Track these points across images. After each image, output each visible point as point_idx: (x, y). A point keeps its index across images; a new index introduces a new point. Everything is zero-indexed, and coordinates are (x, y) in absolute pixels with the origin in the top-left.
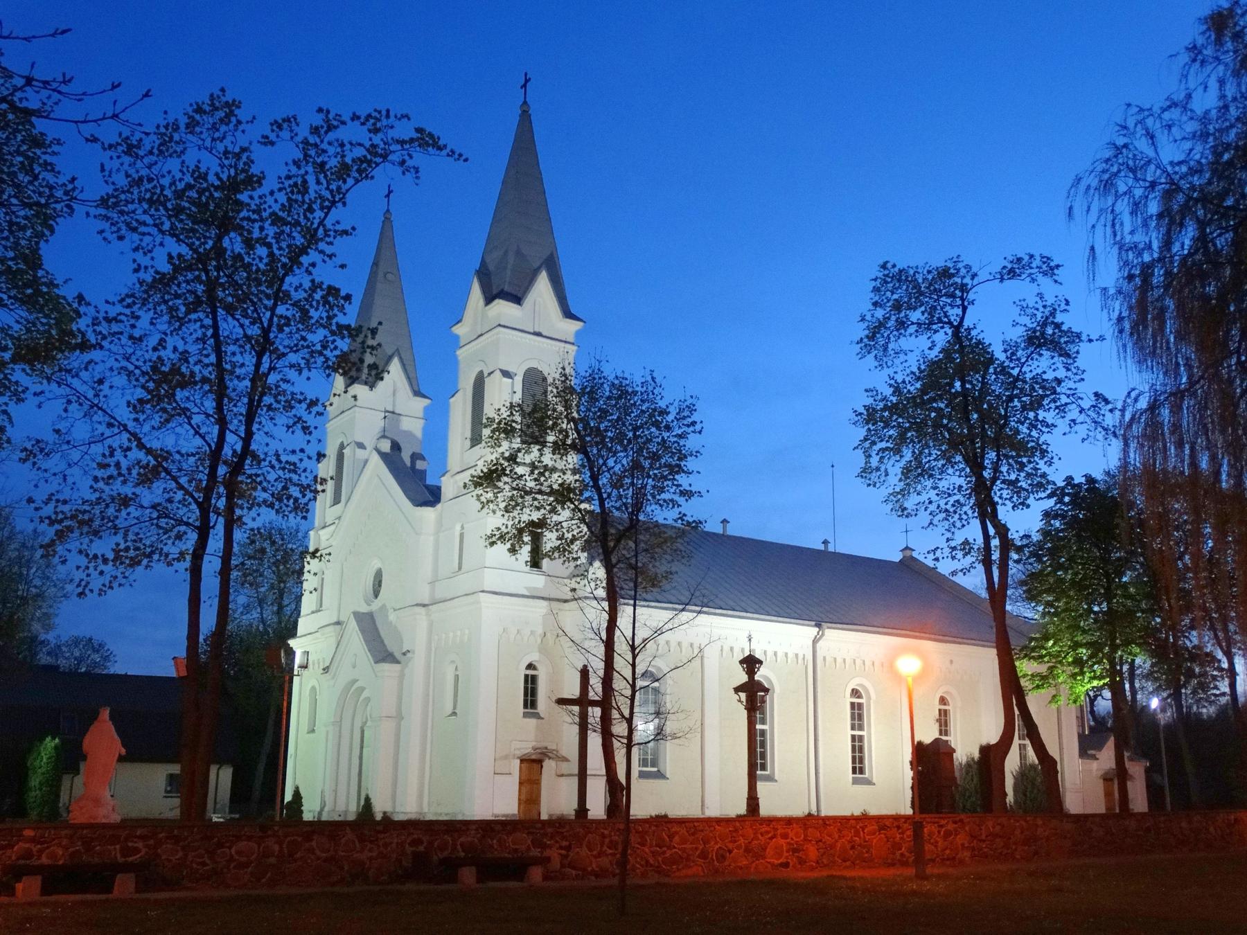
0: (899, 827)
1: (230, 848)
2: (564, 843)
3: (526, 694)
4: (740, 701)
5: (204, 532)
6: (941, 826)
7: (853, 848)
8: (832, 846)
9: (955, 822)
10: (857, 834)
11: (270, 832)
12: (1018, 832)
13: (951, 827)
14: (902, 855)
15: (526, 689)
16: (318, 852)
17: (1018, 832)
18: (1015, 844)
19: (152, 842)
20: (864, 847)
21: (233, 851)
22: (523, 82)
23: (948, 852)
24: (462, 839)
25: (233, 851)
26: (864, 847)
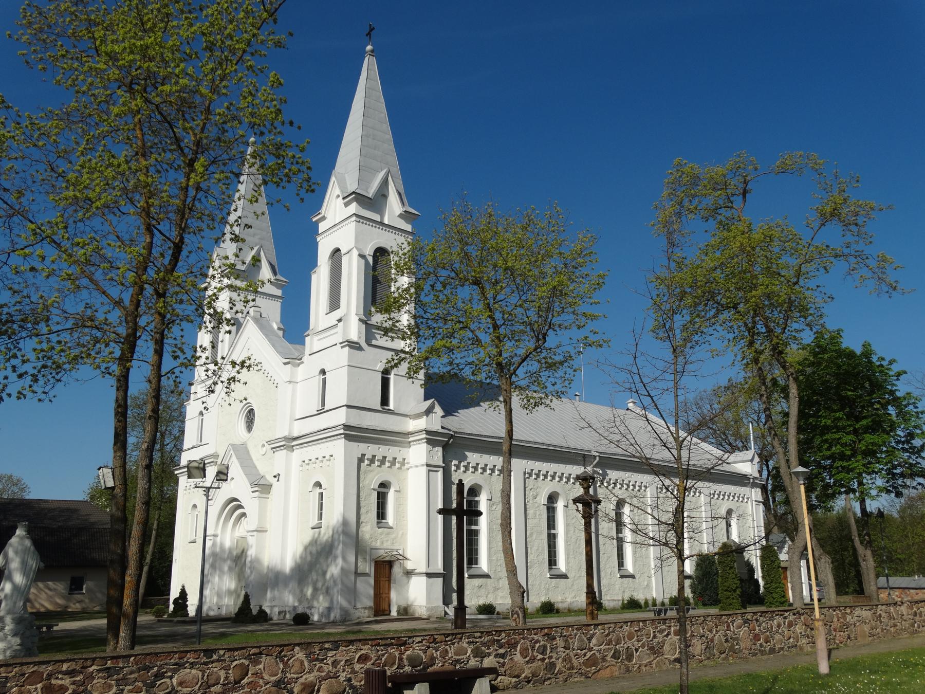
0: (757, 620)
1: (171, 678)
2: (502, 651)
3: (378, 508)
4: (577, 510)
5: (130, 343)
6: (785, 618)
7: (727, 641)
8: (712, 640)
9: (794, 614)
10: (728, 628)
11: (215, 657)
12: (835, 620)
13: (792, 618)
14: (761, 645)
15: (378, 503)
16: (266, 677)
17: (835, 620)
18: (835, 631)
19: (79, 678)
20: (734, 639)
21: (175, 681)
22: (372, 33)
23: (791, 640)
24: (408, 653)
25: (175, 681)
26: (734, 639)
